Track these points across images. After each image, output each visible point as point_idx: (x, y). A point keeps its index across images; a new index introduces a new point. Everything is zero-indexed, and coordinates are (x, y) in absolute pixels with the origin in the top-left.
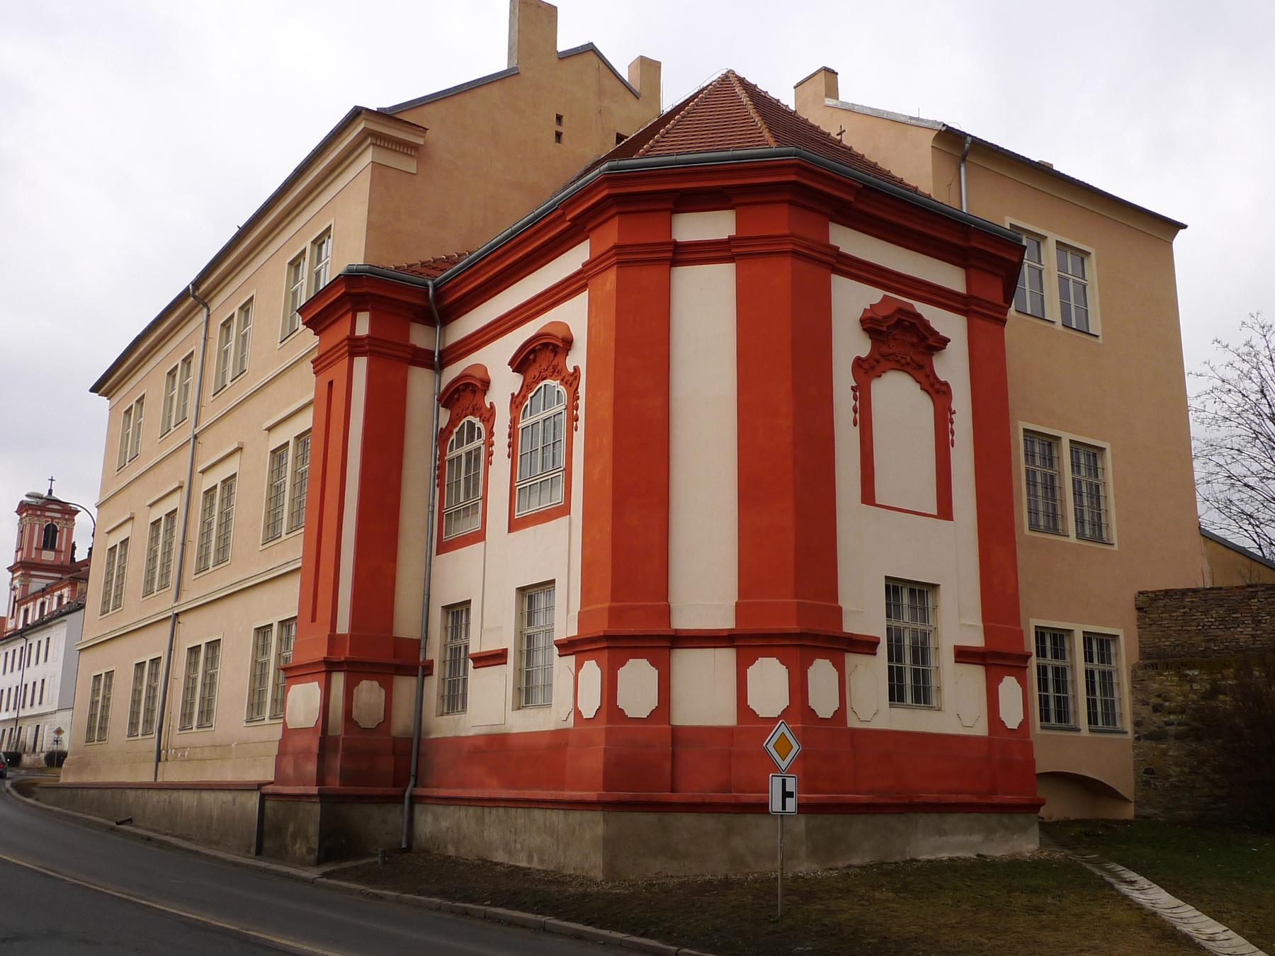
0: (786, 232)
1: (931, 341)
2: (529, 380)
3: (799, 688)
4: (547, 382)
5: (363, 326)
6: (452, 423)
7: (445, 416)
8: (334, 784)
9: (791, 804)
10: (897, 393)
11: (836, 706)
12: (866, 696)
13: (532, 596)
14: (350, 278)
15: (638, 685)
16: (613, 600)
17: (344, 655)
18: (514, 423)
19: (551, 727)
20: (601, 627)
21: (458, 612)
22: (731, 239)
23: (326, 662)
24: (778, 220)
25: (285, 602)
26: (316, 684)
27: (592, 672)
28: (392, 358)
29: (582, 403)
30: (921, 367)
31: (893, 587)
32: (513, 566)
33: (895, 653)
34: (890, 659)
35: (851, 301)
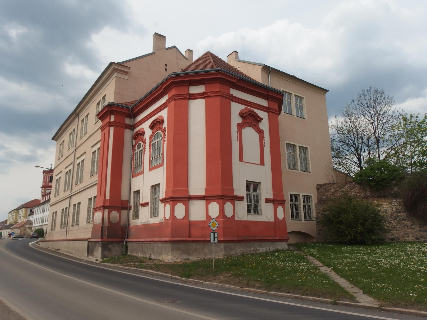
0: (218, 90)
1: (258, 119)
2: (154, 131)
3: (222, 210)
4: (158, 131)
5: (112, 119)
6: (136, 144)
7: (134, 142)
8: (105, 239)
9: (216, 240)
10: (249, 133)
11: (232, 214)
12: (241, 211)
13: (155, 188)
14: (110, 106)
15: (180, 210)
16: (173, 188)
17: (108, 204)
18: (150, 142)
19: (158, 222)
20: (170, 195)
21: (137, 193)
22: (204, 92)
23: (103, 206)
24: (216, 87)
25: (93, 192)
26: (101, 212)
27: (168, 207)
28: (120, 127)
29: (166, 136)
30: (256, 126)
31: (248, 183)
32: (149, 180)
33: (249, 200)
34: (247, 202)
35: (236, 109)
